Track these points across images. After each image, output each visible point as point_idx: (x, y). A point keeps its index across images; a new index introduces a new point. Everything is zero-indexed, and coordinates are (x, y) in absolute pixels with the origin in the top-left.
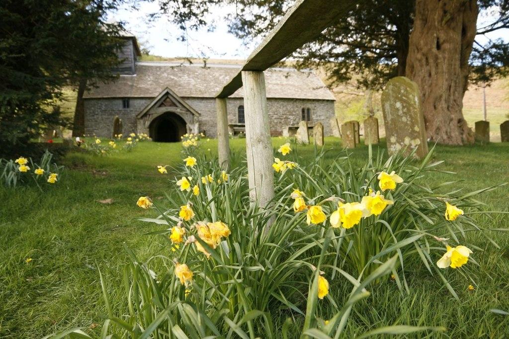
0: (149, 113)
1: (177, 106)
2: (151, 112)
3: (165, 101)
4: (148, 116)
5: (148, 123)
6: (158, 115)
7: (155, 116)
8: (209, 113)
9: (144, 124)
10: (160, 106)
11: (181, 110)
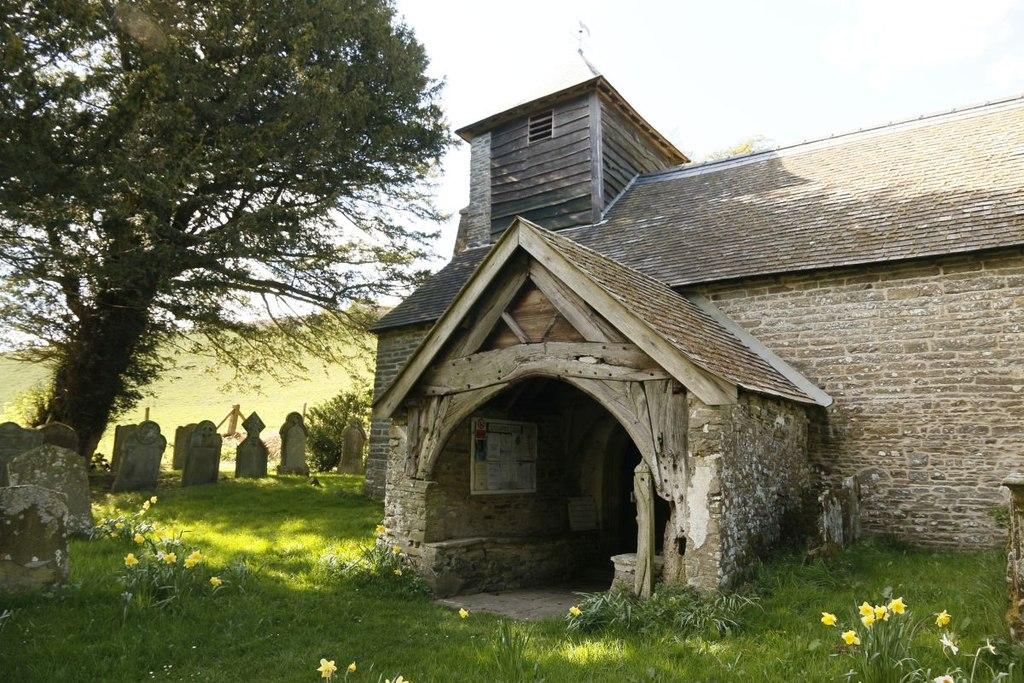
0: (442, 391)
1: (583, 340)
2: (448, 380)
3: (513, 308)
4: (434, 403)
5: (429, 448)
6: (479, 400)
7: (467, 403)
8: (912, 358)
9: (414, 452)
10: (489, 344)
11: (602, 361)
